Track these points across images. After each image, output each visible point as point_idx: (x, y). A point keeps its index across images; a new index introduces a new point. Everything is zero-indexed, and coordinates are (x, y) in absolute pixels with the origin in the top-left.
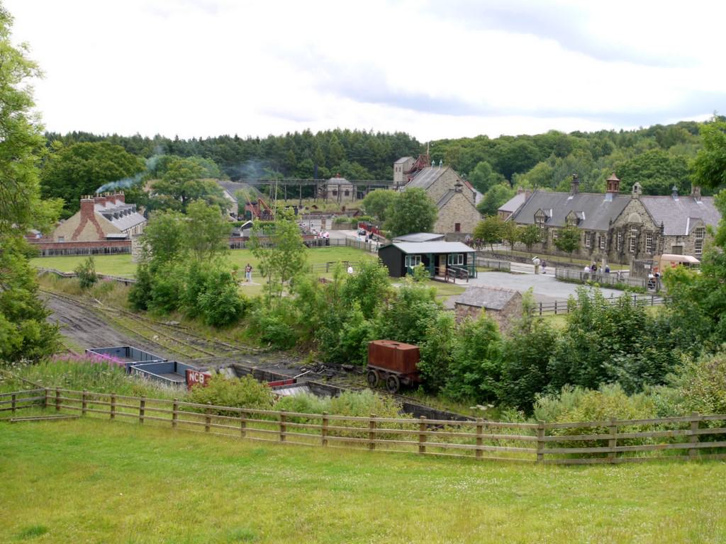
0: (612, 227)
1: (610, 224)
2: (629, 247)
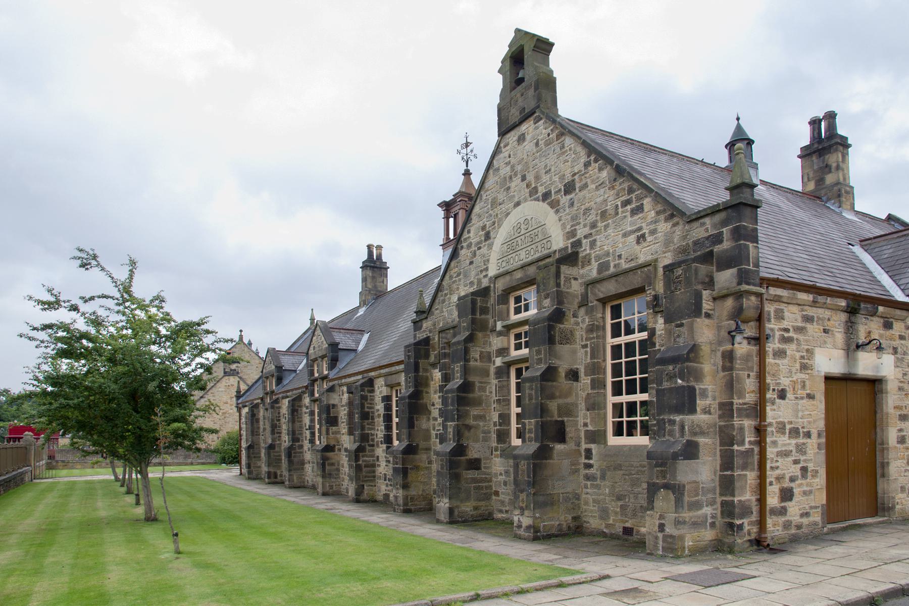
0: (421, 336)
2: (505, 418)
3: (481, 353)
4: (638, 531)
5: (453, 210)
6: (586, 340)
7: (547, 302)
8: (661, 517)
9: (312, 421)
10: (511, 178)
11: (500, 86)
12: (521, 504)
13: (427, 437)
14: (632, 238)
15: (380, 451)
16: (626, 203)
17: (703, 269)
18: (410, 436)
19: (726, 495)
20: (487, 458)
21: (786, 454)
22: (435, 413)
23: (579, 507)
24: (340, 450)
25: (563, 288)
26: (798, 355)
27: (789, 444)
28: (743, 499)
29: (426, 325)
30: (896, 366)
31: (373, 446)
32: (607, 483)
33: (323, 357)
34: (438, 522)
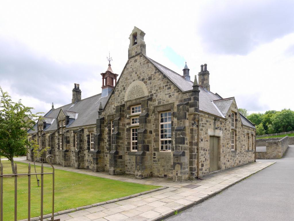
0: (101, 117)
1: (100, 113)
2: (129, 143)
3: (123, 124)
4: (168, 176)
5: (105, 76)
6: (154, 122)
7: (144, 111)
8: (177, 171)
9: (59, 141)
10: (132, 72)
11: (129, 43)
12: (138, 169)
13: (103, 148)
14: (168, 96)
15: (86, 152)
16: (166, 86)
17: (187, 107)
18: (98, 148)
19: (191, 166)
20: (124, 155)
21: (202, 155)
22: (106, 141)
23: (152, 169)
24: (70, 152)
25: (149, 107)
26: (205, 130)
27: (203, 153)
28: (194, 166)
29: (103, 113)
30: (222, 134)
31: (83, 150)
32: (159, 162)
33: (63, 120)
34: (110, 174)
